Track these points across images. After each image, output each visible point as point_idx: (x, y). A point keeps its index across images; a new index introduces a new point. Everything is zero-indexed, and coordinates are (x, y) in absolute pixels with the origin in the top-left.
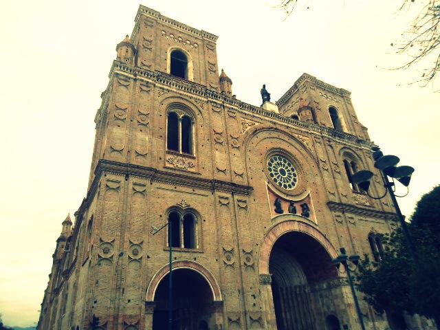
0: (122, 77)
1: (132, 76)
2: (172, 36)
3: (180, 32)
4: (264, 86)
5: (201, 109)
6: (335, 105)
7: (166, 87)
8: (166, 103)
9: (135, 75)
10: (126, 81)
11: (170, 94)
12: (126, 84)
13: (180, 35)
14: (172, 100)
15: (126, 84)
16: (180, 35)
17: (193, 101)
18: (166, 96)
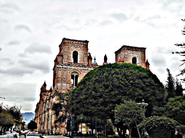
0: (59, 68)
1: (61, 67)
2: (73, 46)
3: (76, 44)
4: (106, 55)
5: (80, 72)
6: (136, 56)
7: (71, 67)
8: (71, 73)
9: (62, 66)
10: (60, 68)
11: (72, 69)
12: (60, 69)
13: (76, 45)
14: (72, 71)
15: (60, 69)
16: (76, 45)
17: (78, 70)
18: (71, 70)
